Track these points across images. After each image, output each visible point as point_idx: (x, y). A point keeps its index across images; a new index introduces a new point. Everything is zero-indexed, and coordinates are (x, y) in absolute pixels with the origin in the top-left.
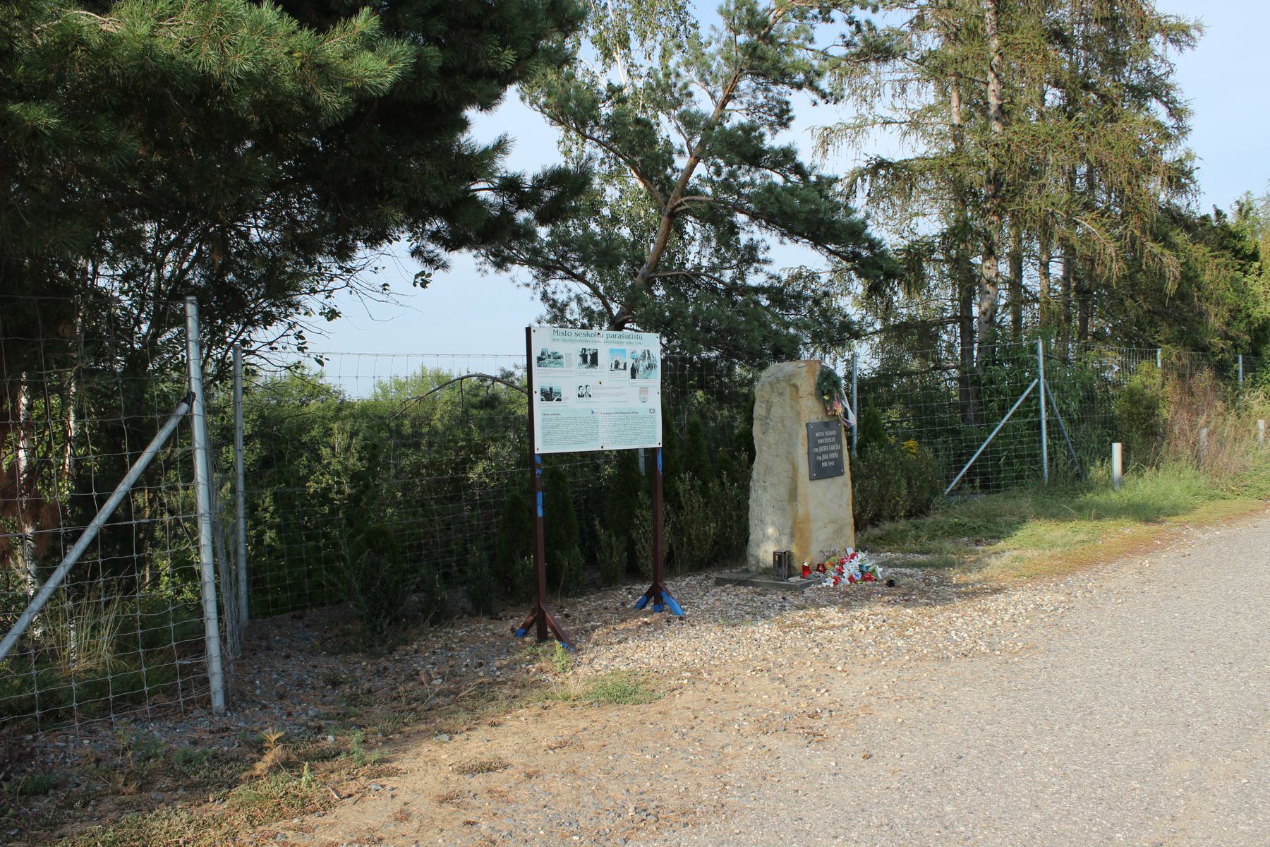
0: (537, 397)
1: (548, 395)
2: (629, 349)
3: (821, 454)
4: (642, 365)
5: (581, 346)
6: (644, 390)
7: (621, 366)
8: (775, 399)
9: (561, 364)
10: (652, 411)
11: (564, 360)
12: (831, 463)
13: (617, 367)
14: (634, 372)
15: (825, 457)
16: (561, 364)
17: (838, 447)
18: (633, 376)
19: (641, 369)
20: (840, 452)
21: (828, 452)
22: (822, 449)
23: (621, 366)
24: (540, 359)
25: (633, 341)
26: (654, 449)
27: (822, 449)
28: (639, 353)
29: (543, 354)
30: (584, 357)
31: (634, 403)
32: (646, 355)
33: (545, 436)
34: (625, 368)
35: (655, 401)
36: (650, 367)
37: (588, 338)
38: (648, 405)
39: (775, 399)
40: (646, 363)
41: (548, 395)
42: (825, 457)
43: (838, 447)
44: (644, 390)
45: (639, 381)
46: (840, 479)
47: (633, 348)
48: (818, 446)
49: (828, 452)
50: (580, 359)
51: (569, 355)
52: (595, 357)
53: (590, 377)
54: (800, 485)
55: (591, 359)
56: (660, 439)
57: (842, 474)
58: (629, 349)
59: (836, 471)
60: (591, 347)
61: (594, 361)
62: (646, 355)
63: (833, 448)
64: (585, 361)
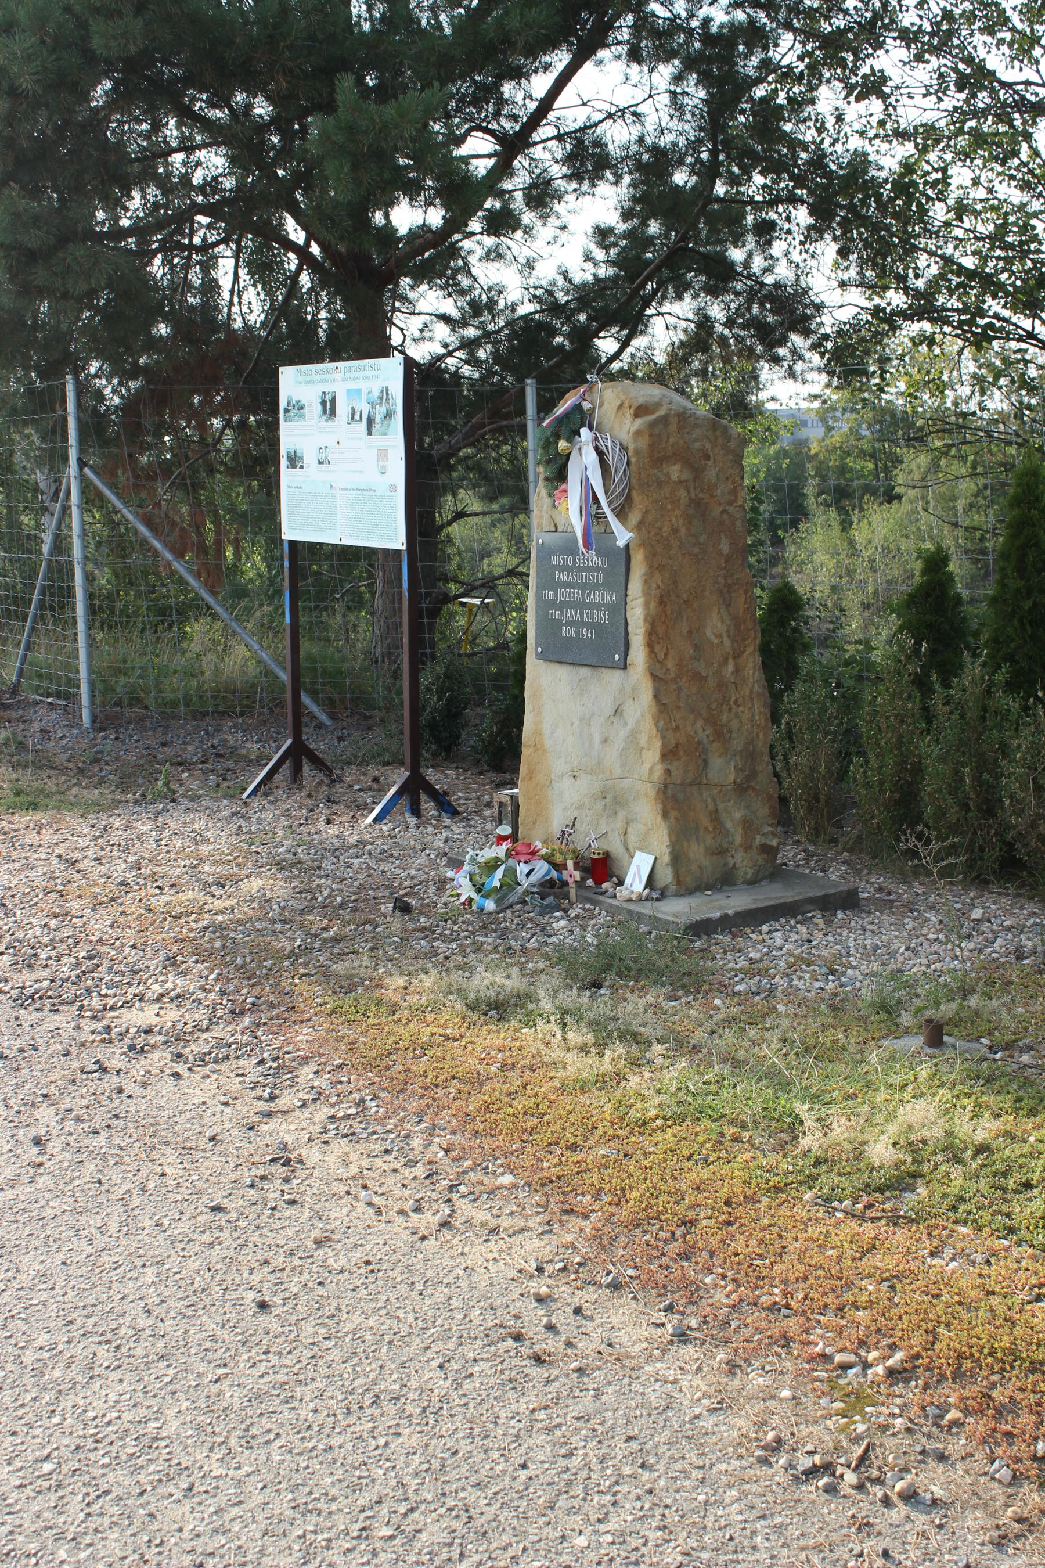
0: (284, 462)
2: (364, 386)
6: (383, 453)
7: (357, 417)
10: (393, 488)
11: (306, 411)
12: (587, 633)
15: (573, 614)
16: (302, 416)
17: (611, 598)
18: (370, 433)
19: (378, 419)
21: (580, 606)
22: (563, 595)
25: (369, 374)
27: (563, 595)
28: (376, 393)
30: (323, 403)
33: (291, 514)
36: (389, 415)
37: (328, 376)
42: (573, 614)
43: (611, 598)
44: (383, 453)
45: (377, 440)
46: (615, 677)
49: (580, 606)
50: (320, 408)
52: (333, 401)
56: (403, 538)
60: (328, 388)
62: (385, 395)
63: (596, 597)
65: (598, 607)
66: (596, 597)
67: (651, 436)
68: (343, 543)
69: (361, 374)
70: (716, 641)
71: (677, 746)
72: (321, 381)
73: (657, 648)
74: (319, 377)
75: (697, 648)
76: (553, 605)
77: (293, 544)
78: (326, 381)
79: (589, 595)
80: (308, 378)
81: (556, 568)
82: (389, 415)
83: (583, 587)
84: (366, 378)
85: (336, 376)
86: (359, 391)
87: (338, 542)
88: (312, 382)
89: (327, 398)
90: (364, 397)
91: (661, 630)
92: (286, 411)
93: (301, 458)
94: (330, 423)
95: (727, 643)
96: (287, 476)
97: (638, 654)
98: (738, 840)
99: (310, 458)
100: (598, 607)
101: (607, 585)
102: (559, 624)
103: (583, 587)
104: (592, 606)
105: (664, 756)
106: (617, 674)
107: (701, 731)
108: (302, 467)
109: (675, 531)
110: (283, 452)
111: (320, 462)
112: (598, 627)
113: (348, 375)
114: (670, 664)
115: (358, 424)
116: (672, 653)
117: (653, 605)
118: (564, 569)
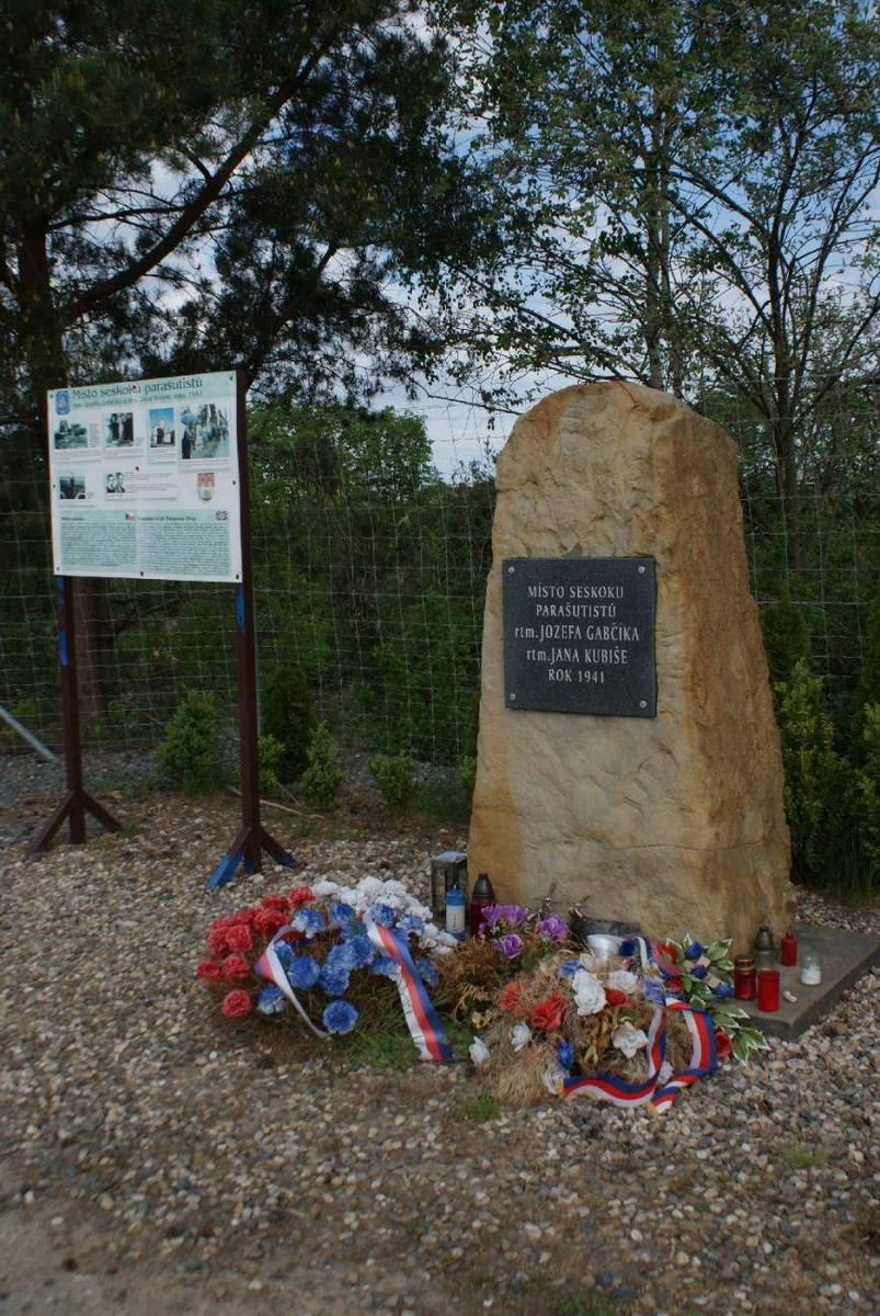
0: (55, 493)
2: (178, 406)
3: (549, 645)
5: (110, 411)
6: (206, 478)
7: (167, 439)
9: (83, 442)
10: (222, 515)
11: (88, 436)
16: (83, 442)
18: (186, 454)
19: (199, 440)
21: (580, 644)
22: (548, 632)
27: (548, 632)
28: (195, 411)
29: (62, 428)
30: (114, 427)
31: (187, 499)
32: (209, 414)
33: (67, 547)
34: (172, 442)
35: (228, 495)
37: (119, 397)
38: (216, 505)
40: (208, 429)
44: (206, 478)
45: (198, 464)
47: (184, 404)
48: (538, 622)
49: (580, 644)
50: (108, 433)
51: (94, 426)
52: (129, 424)
53: (121, 460)
55: (122, 431)
57: (650, 714)
60: (122, 410)
62: (209, 414)
63: (606, 633)
64: (115, 435)
65: (609, 645)
66: (606, 633)
67: (675, 442)
68: (145, 577)
69: (173, 392)
70: (739, 677)
71: (723, 803)
72: (111, 403)
73: (699, 690)
74: (107, 398)
75: (727, 686)
76: (533, 644)
77: (68, 580)
78: (117, 402)
79: (593, 631)
80: (89, 400)
81: (538, 600)
82: (217, 435)
83: (583, 622)
84: (180, 396)
85: (134, 395)
86: (169, 412)
87: (139, 577)
88: (96, 404)
89: (119, 420)
90: (177, 417)
91: (700, 668)
92: (58, 437)
93: (82, 487)
94: (124, 448)
95: (747, 678)
96: (58, 506)
97: (673, 698)
98: (771, 901)
99: (94, 484)
100: (609, 645)
101: (623, 619)
102: (544, 667)
103: (583, 622)
104: (599, 644)
105: (715, 817)
106: (646, 723)
107: (735, 782)
108: (82, 497)
109: (702, 553)
110: (54, 481)
111: (109, 491)
112: (611, 670)
113: (150, 394)
114: (709, 709)
115: (168, 450)
116: (711, 695)
117: (692, 641)
118: (548, 602)
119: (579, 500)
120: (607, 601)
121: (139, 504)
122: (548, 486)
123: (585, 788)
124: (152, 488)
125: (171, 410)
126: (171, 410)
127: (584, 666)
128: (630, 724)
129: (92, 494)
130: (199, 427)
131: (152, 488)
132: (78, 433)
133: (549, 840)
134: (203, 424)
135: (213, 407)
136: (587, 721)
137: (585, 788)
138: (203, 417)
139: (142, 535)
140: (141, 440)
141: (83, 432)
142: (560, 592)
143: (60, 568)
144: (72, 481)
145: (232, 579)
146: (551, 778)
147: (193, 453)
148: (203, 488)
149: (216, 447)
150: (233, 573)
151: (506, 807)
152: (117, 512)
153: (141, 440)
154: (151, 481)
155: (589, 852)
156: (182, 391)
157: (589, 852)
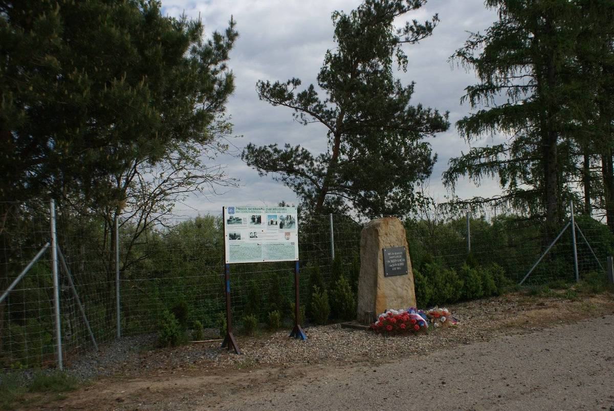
0: (227, 238)
1: (233, 237)
4: (286, 222)
6: (288, 234)
8: (369, 237)
9: (241, 223)
10: (293, 243)
11: (242, 221)
12: (398, 268)
13: (272, 222)
14: (282, 226)
16: (241, 223)
17: (404, 260)
19: (286, 224)
20: (405, 263)
23: (275, 223)
24: (228, 221)
26: (295, 262)
29: (231, 218)
30: (253, 219)
34: (276, 224)
38: (291, 241)
39: (369, 237)
41: (233, 237)
45: (285, 230)
50: (251, 220)
51: (245, 219)
53: (257, 228)
54: (379, 280)
58: (279, 215)
59: (402, 272)
61: (259, 220)
82: (292, 223)
93: (239, 236)
94: (257, 225)
108: (240, 239)
111: (251, 237)
112: (401, 266)
115: (276, 226)
119: (393, 238)
120: (400, 255)
121: (263, 240)
122: (388, 235)
123: (399, 289)
124: (268, 236)
125: (276, 216)
126: (276, 216)
127: (397, 266)
128: (404, 276)
129: (244, 238)
130: (286, 221)
131: (268, 236)
132: (238, 220)
133: (393, 300)
134: (287, 220)
135: (290, 216)
136: (398, 277)
137: (399, 289)
138: (287, 218)
139: (263, 249)
140: (264, 223)
141: (240, 220)
142: (393, 254)
143: (229, 260)
144: (235, 234)
145: (296, 260)
146: (394, 289)
147: (283, 227)
148: (287, 236)
149: (291, 226)
150: (296, 258)
151: (385, 297)
152: (254, 244)
153: (264, 223)
154: (267, 235)
155: (400, 300)
156: (280, 211)
157: (400, 300)
